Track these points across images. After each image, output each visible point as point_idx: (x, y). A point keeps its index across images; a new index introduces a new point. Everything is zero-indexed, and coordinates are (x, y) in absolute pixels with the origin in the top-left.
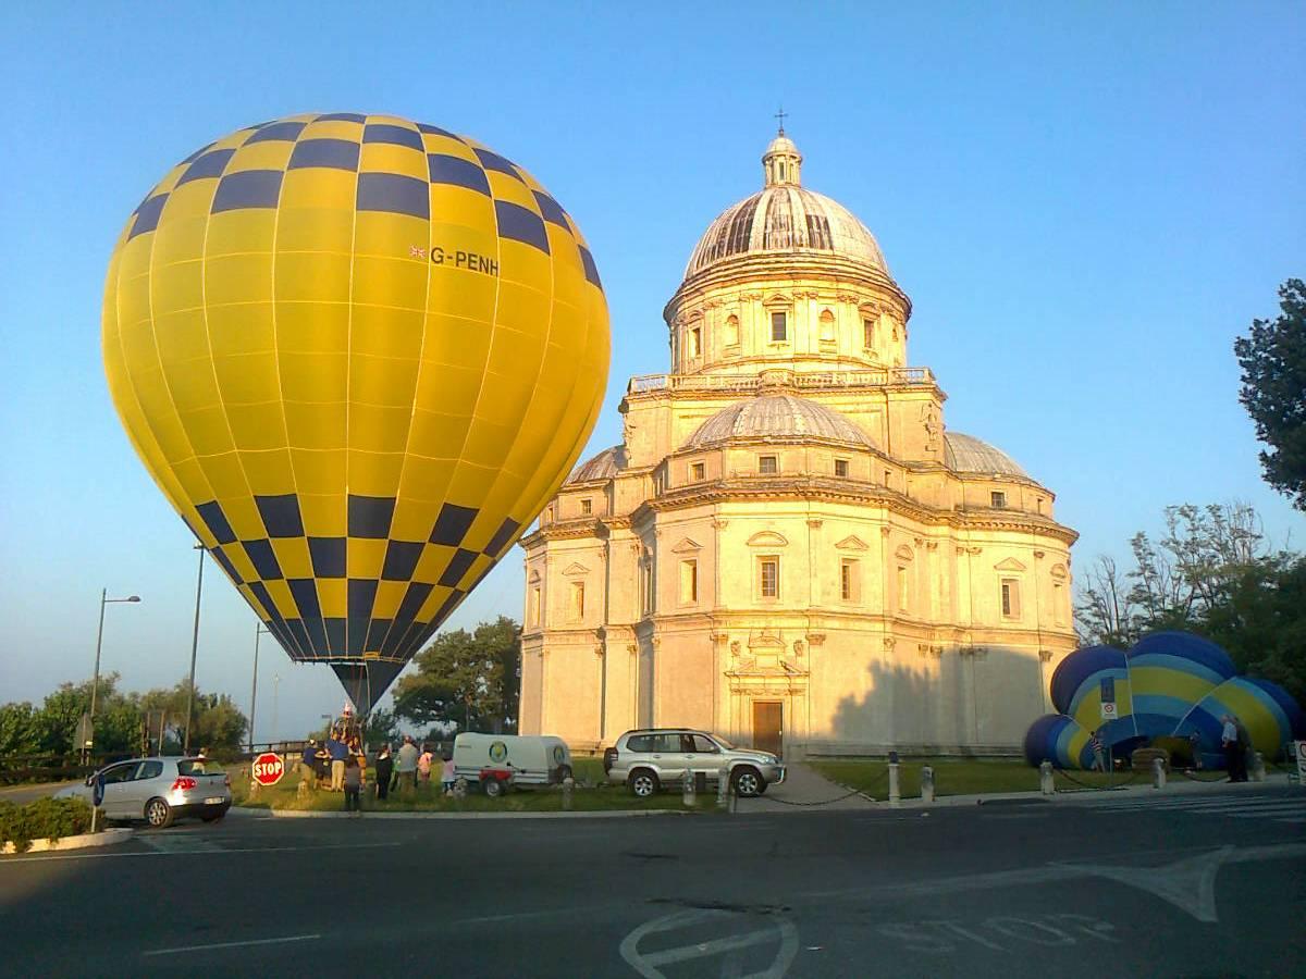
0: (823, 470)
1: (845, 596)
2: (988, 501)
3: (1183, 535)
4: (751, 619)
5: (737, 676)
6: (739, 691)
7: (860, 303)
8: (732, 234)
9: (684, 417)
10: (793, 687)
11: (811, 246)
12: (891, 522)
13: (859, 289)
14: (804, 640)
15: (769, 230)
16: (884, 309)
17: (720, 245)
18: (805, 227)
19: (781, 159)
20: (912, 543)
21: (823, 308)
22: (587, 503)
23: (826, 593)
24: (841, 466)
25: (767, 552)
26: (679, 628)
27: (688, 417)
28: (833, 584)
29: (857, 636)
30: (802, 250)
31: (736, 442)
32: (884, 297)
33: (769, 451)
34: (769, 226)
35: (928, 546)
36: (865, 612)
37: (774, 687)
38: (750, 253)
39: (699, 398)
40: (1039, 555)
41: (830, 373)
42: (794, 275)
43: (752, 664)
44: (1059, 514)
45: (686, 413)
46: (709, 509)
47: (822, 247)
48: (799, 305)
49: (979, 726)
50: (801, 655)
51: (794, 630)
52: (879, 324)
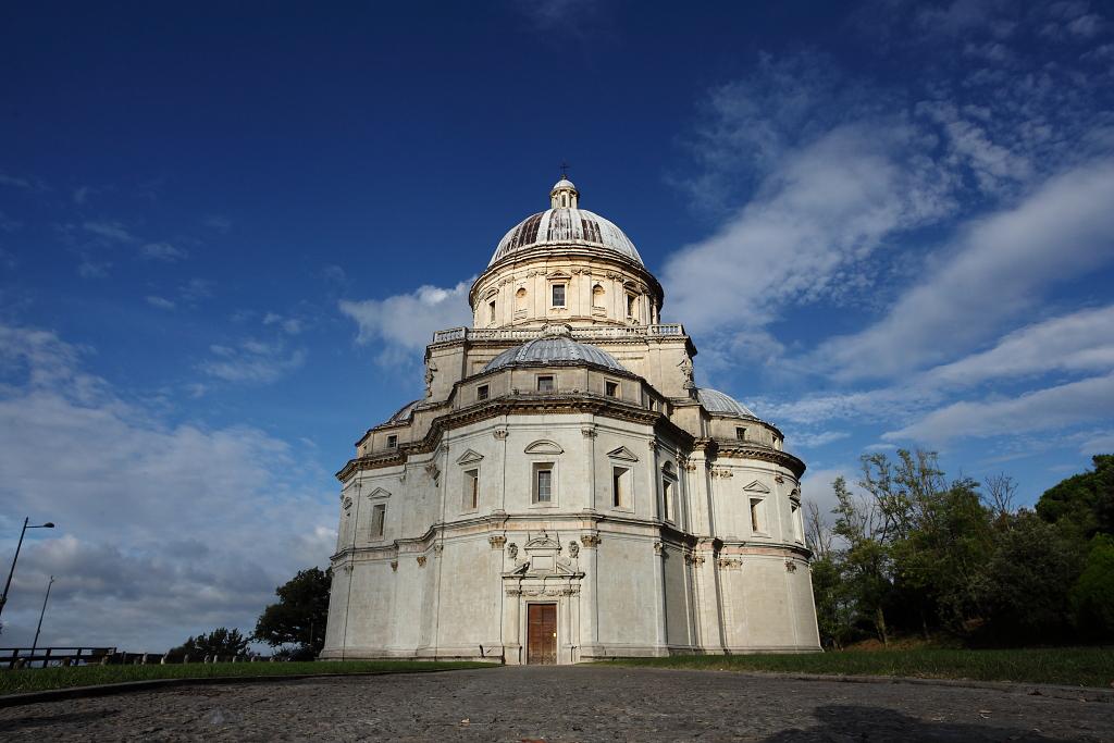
1: (617, 503)
2: (734, 435)
3: (877, 479)
4: (526, 522)
7: (626, 280)
8: (524, 232)
11: (586, 239)
14: (579, 542)
15: (552, 228)
16: (644, 292)
17: (514, 241)
18: (580, 226)
19: (563, 193)
20: (674, 463)
22: (392, 439)
24: (611, 387)
26: (460, 534)
28: (605, 490)
29: (629, 539)
30: (578, 241)
31: (516, 366)
34: (553, 225)
38: (537, 243)
39: (490, 347)
40: (780, 480)
42: (570, 257)
43: (525, 569)
45: (479, 358)
46: (490, 422)
47: (594, 240)
48: (575, 278)
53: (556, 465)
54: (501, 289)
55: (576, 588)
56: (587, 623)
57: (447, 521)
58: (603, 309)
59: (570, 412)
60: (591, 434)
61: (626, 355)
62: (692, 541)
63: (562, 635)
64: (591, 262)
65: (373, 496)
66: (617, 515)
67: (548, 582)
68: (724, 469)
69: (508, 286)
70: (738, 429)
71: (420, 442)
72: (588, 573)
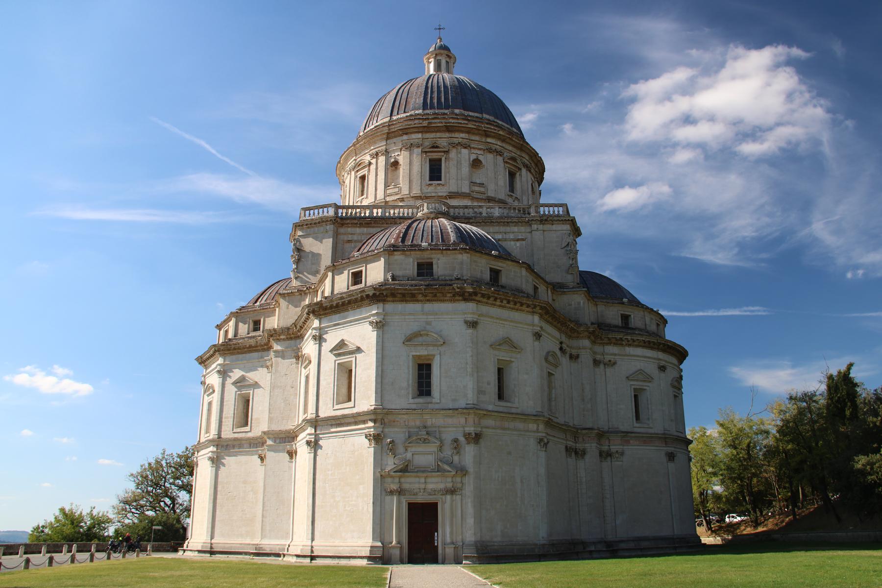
0: (479, 275)
1: (501, 396)
2: (618, 322)
5: (392, 477)
6: (391, 493)
9: (349, 241)
10: (450, 485)
12: (541, 328)
13: (504, 145)
14: (462, 439)
16: (526, 166)
19: (438, 58)
20: (558, 353)
21: (473, 157)
23: (480, 392)
25: (422, 352)
27: (349, 241)
32: (524, 155)
33: (426, 256)
35: (571, 357)
36: (519, 411)
37: (430, 486)
40: (662, 368)
41: (480, 207)
42: (449, 129)
44: (671, 334)
45: (350, 237)
48: (453, 154)
49: (618, 522)
50: (458, 453)
51: (454, 428)
52: (520, 175)
53: (437, 358)
54: (374, 161)
55: (459, 485)
56: (470, 521)
57: (322, 415)
58: (481, 185)
59: (453, 300)
60: (473, 325)
61: (507, 236)
62: (575, 432)
63: (444, 535)
64: (468, 133)
65: (240, 383)
66: (501, 409)
67: (429, 480)
68: (608, 358)
69: (382, 159)
70: (622, 315)
71: (288, 329)
72: (471, 470)
